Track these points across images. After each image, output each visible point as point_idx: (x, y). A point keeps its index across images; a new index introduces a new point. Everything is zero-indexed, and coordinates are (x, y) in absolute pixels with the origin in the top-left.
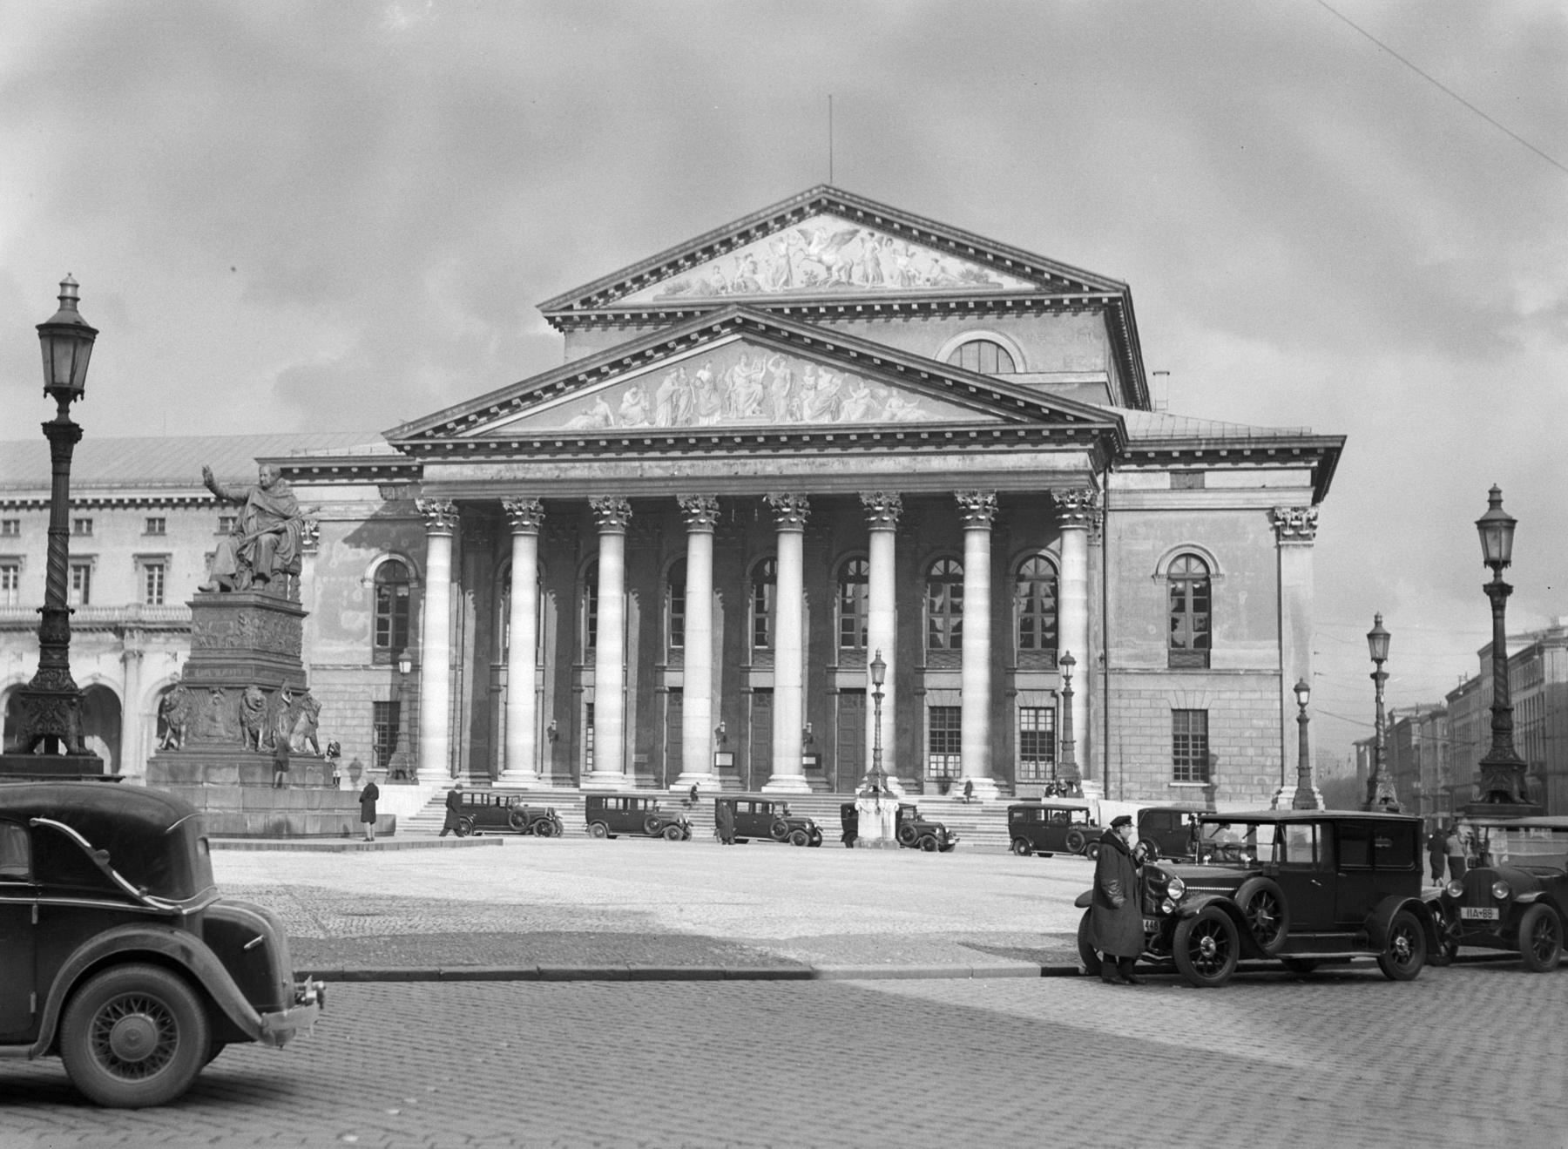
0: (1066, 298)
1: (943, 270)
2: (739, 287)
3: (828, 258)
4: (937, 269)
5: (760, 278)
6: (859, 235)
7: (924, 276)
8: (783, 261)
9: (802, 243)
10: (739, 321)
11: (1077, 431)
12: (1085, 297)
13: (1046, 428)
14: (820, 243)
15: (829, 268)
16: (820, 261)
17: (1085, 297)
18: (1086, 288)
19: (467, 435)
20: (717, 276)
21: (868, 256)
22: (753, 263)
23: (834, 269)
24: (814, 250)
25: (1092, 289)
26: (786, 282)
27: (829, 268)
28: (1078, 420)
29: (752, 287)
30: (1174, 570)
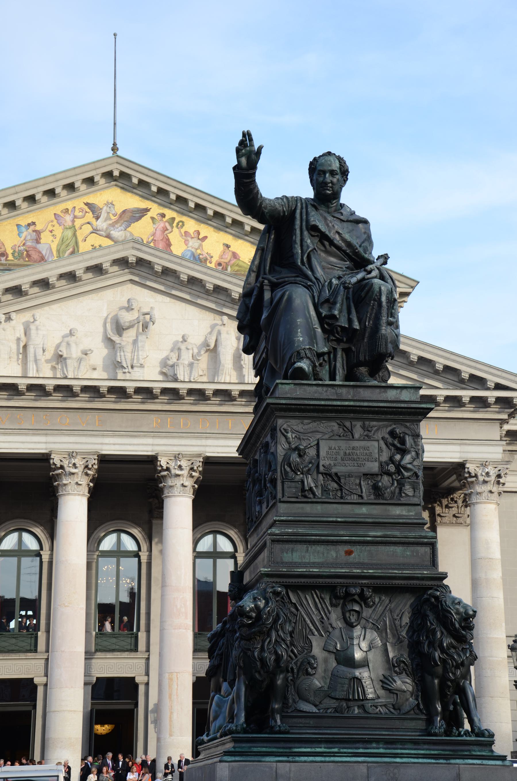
1: (235, 255)
2: (21, 253)
3: (117, 233)
4: (228, 256)
5: (43, 248)
6: (150, 214)
7: (215, 260)
8: (69, 233)
9: (90, 216)
10: (132, 259)
11: (499, 400)
13: (466, 394)
14: (108, 218)
21: (159, 236)
22: (38, 233)
24: (101, 224)
28: (499, 387)
29: (35, 256)
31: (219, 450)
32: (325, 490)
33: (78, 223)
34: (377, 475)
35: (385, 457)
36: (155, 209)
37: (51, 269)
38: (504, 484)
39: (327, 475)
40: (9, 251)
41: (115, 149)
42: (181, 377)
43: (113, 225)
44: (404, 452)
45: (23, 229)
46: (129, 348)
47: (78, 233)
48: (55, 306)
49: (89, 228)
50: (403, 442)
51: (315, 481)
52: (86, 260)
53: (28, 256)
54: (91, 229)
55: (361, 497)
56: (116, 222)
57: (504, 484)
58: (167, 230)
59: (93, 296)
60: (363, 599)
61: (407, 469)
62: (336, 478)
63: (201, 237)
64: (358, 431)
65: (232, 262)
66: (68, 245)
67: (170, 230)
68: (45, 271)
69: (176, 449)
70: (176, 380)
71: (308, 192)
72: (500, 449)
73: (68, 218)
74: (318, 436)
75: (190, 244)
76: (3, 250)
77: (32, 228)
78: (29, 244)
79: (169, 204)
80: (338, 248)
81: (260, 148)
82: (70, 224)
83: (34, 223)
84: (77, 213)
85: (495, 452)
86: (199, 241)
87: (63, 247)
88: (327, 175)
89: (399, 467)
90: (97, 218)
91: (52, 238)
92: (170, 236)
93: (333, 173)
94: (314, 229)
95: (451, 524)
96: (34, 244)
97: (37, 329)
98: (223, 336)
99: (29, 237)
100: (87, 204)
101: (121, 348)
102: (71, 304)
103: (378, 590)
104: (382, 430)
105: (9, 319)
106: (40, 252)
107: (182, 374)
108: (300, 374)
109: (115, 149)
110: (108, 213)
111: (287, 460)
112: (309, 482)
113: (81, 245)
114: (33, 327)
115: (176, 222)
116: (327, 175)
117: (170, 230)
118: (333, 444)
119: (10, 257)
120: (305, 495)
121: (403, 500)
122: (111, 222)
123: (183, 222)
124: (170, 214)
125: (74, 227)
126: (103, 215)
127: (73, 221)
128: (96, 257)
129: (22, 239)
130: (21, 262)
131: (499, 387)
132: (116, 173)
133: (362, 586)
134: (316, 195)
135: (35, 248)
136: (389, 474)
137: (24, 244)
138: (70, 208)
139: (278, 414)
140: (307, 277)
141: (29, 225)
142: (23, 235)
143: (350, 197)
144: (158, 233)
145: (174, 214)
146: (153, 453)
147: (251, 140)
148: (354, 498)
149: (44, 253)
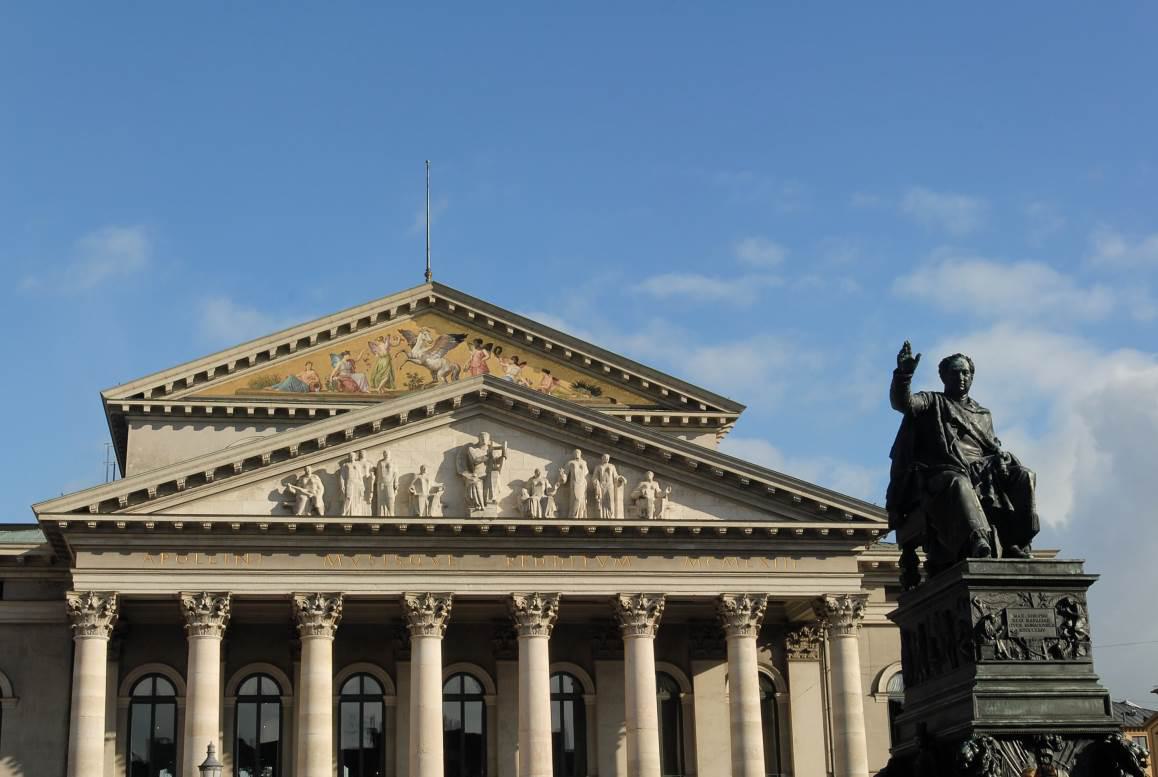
0: (686, 417)
3: (433, 361)
5: (358, 378)
8: (384, 362)
12: (704, 417)
13: (825, 526)
15: (434, 372)
16: (424, 364)
17: (704, 417)
18: (703, 408)
19: (143, 513)
20: (309, 373)
21: (476, 362)
23: (440, 373)
24: (417, 352)
25: (709, 409)
26: (388, 384)
27: (434, 372)
28: (857, 519)
29: (350, 386)
30: (890, 689)
31: (576, 588)
32: (1014, 653)
33: (393, 351)
34: (1055, 639)
35: (1060, 620)
36: (473, 335)
37: (402, 406)
38: (862, 617)
39: (1016, 640)
40: (323, 382)
41: (427, 275)
42: (534, 514)
43: (428, 352)
44: (1075, 618)
45: (338, 359)
46: (480, 485)
47: (393, 362)
48: (405, 443)
49: (404, 357)
50: (1074, 608)
51: (1006, 645)
52: (437, 396)
53: (343, 386)
54: (405, 357)
55: (1044, 658)
56: (432, 350)
57: (862, 617)
58: (484, 356)
59: (439, 432)
60: (1055, 747)
61: (1080, 633)
62: (1021, 642)
63: (520, 362)
64: (1036, 600)
65: (552, 389)
66: (382, 375)
67: (488, 356)
68: (396, 407)
69: (531, 589)
70: (529, 516)
71: (940, 387)
72: (859, 582)
73: (383, 347)
74: (1004, 606)
75: (509, 370)
76: (317, 380)
77: (346, 357)
78: (343, 373)
79: (487, 330)
80: (979, 442)
81: (918, 356)
82: (385, 352)
83: (348, 353)
84: (392, 342)
85: (854, 586)
86: (518, 367)
87: (378, 376)
88: (953, 373)
89: (1072, 630)
90: (413, 346)
91: (367, 367)
92: (488, 362)
93: (965, 372)
94: (955, 422)
95: (801, 660)
96: (349, 375)
97: (387, 467)
98: (577, 469)
99: (343, 368)
100: (401, 331)
101: (473, 485)
102: (421, 439)
103: (1066, 737)
104: (1053, 598)
105: (360, 457)
106: (354, 382)
107: (535, 509)
108: (983, 552)
109: (427, 275)
110: (424, 340)
111: (981, 624)
112: (1001, 645)
113: (397, 374)
114: (383, 464)
115: (493, 347)
116: (953, 373)
117: (488, 356)
118: (1017, 612)
119: (324, 388)
120: (1000, 658)
121: (1078, 659)
122: (426, 349)
123: (501, 348)
124: (486, 340)
125: (389, 355)
126: (419, 342)
127: (388, 349)
128: (448, 392)
129: (336, 369)
130: (336, 392)
131: (857, 519)
132: (432, 300)
133: (1054, 734)
134: (945, 390)
135: (349, 378)
136: (1064, 637)
137: (338, 375)
138: (385, 335)
139: (970, 587)
140: (957, 464)
141: (343, 354)
142: (337, 365)
143: (975, 393)
144: (476, 359)
145: (492, 341)
146: (508, 593)
147: (909, 349)
148: (1038, 659)
149: (358, 383)
